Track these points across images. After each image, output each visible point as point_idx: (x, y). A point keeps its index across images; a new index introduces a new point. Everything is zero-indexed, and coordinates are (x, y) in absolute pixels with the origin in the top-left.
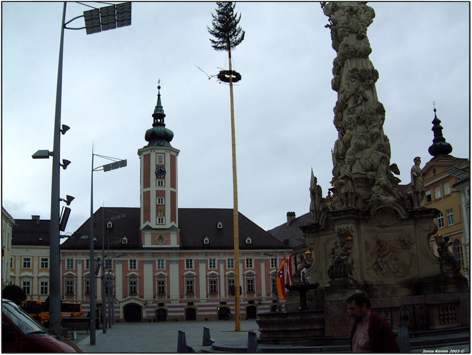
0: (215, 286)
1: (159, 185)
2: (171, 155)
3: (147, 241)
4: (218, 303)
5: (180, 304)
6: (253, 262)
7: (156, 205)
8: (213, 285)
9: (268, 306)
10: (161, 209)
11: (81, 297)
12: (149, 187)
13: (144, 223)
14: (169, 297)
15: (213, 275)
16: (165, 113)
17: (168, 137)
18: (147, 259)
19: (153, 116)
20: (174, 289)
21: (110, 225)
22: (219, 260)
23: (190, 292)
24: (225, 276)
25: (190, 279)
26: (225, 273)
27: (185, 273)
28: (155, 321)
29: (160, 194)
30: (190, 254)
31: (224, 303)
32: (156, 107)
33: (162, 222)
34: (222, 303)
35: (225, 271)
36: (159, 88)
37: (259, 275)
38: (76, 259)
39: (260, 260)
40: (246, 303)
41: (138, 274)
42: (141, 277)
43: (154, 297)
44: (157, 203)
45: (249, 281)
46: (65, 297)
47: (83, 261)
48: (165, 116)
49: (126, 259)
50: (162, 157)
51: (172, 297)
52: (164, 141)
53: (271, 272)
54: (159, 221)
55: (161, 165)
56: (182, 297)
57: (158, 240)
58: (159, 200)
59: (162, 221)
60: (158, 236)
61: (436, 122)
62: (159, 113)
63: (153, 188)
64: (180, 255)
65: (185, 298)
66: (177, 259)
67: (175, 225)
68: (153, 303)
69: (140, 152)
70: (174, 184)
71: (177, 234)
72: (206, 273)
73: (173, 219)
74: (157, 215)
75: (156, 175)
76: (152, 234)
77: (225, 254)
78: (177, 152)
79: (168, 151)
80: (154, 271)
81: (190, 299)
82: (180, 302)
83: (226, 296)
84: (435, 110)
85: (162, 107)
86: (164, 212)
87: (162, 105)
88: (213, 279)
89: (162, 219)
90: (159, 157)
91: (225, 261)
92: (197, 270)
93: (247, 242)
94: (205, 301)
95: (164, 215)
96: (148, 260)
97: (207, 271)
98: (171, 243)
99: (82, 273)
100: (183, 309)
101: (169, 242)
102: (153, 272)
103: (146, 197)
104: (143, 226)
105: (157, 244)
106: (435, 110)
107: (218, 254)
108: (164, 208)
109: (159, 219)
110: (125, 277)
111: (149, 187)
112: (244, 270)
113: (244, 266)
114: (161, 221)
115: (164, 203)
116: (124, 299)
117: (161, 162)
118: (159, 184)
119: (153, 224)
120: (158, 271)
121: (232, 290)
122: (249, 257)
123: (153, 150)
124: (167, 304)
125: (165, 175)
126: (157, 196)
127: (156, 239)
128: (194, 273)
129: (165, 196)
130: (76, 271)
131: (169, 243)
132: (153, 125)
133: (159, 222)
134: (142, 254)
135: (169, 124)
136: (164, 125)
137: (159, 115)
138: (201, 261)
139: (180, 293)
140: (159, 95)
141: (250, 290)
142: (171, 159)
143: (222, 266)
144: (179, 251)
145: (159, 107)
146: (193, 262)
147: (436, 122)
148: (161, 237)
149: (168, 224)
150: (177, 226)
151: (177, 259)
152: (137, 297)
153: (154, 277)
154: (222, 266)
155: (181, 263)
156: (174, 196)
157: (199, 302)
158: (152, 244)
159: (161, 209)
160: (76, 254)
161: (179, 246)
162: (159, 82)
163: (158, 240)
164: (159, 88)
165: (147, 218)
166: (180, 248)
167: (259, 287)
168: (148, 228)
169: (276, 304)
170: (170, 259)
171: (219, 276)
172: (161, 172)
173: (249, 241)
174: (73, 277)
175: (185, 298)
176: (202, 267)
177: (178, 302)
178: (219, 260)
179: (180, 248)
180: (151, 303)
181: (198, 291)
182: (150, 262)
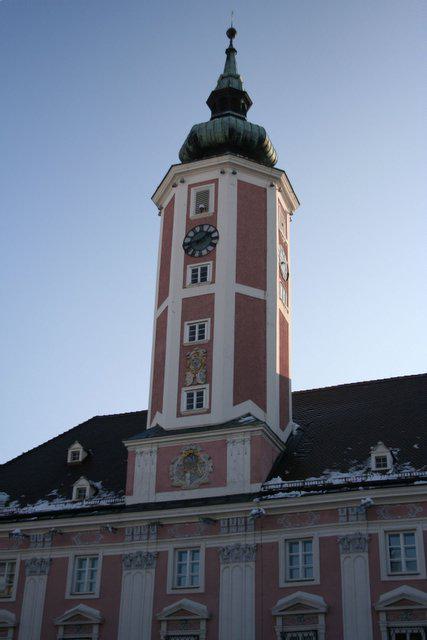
1: (194, 281)
33: (200, 405)
36: (231, 33)
41: (96, 612)
44: (186, 340)
50: (207, 193)
54: (190, 401)
58: (192, 328)
59: (200, 400)
63: (177, 294)
67: (257, 412)
72: (374, 598)
74: (182, 383)
75: (186, 251)
85: (238, 77)
87: (239, 72)
89: (200, 394)
90: (199, 195)
95: (208, 379)
96: (140, 554)
97: (377, 586)
98: (231, 475)
101: (219, 478)
105: (178, 488)
109: (190, 395)
114: (196, 402)
118: (194, 276)
125: (214, 245)
126: (184, 319)
127: (174, 469)
129: (211, 315)
131: (223, 482)
133: (190, 407)
134: (116, 533)
137: (229, 99)
140: (231, 51)
145: (230, 74)
151: (251, 540)
164: (231, 33)
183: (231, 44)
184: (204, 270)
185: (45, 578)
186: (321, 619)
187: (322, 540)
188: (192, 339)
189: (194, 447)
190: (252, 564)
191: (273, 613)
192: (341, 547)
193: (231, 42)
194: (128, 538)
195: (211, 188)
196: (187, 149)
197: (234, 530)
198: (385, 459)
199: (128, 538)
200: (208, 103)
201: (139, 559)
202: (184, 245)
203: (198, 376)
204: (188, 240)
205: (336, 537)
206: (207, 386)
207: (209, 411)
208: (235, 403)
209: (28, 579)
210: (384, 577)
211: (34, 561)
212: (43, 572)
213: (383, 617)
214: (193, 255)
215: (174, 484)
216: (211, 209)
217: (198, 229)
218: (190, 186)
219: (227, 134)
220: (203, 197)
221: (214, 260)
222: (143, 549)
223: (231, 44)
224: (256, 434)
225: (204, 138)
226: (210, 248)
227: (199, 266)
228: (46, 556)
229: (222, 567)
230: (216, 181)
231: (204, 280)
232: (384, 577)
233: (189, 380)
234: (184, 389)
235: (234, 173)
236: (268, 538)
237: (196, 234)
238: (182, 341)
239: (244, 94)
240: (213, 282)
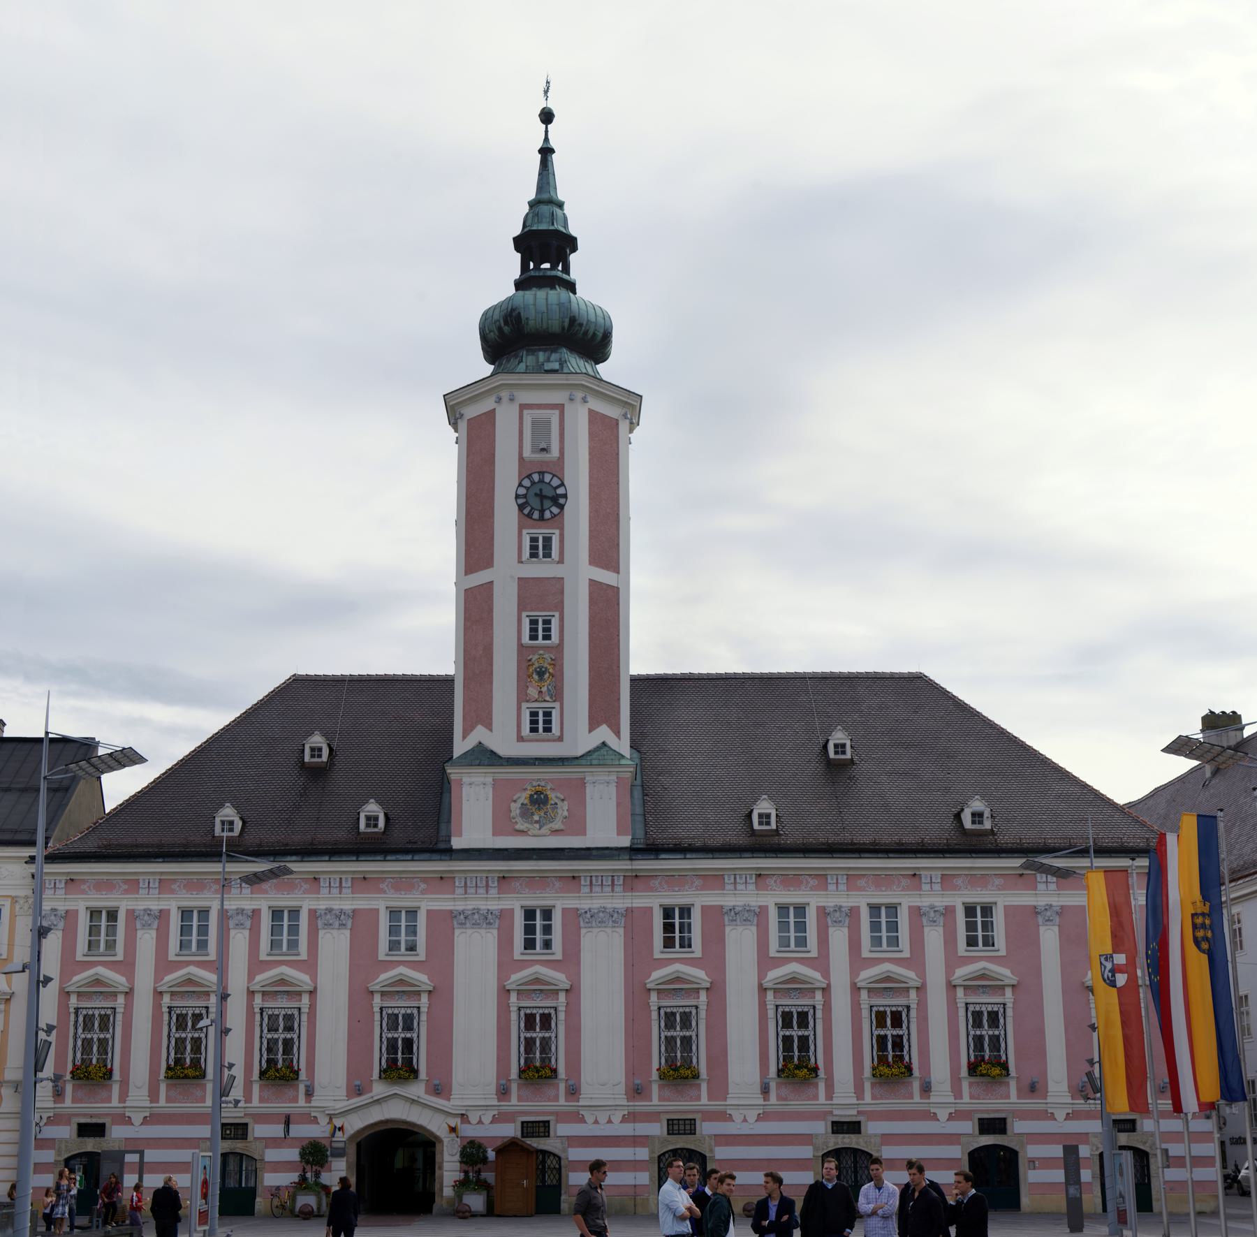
0: (804, 1041)
1: (534, 555)
2: (591, 411)
3: (475, 815)
4: (820, 1127)
5: (627, 1129)
6: (999, 919)
7: (521, 646)
8: (795, 1033)
10: (541, 671)
11: (145, 1091)
12: (489, 563)
13: (464, 737)
14: (573, 1092)
15: (793, 985)
16: (573, 230)
17: (591, 341)
18: (470, 905)
19: (519, 243)
20: (602, 1051)
21: (316, 751)
22: (823, 912)
23: (679, 1072)
24: (856, 989)
25: (676, 1003)
26: (854, 972)
27: (657, 975)
28: (482, 1216)
29: (541, 600)
30: (675, 880)
31: (853, 1127)
32: (532, 204)
33: (548, 729)
34: (839, 1127)
35: (857, 961)
36: (547, 117)
37: (1029, 987)
38: (132, 905)
39: (1035, 911)
41: (423, 978)
42: (442, 993)
43: (503, 1092)
44: (526, 639)
45: (977, 1016)
46: (69, 1089)
47: (163, 915)
48: (570, 243)
49: (373, 904)
50: (548, 422)
51: (591, 1092)
52: (565, 353)
54: (534, 722)
55: (543, 463)
56: (637, 1091)
57: (526, 813)
58: (534, 622)
59: (548, 722)
60: (523, 797)
62: (543, 227)
64: (633, 881)
65: (655, 1101)
66: (621, 901)
68: (494, 1120)
69: (455, 405)
70: (608, 547)
71: (619, 782)
72: (762, 974)
73: (602, 712)
74: (522, 697)
75: (521, 508)
76: (496, 784)
77: (852, 879)
78: (630, 403)
79: (579, 395)
80: (506, 964)
81: (680, 1106)
82: (631, 1117)
83: (859, 1092)
85: (560, 205)
86: (558, 677)
87: (561, 196)
88: (794, 1003)
89: (548, 714)
90: (534, 423)
91: (853, 912)
92: (715, 958)
93: (968, 824)
94: (752, 1115)
95: (557, 695)
96: (476, 911)
97: (765, 962)
99: (158, 977)
100: (643, 1154)
102: (500, 965)
103: (475, 610)
104: (460, 746)
105: (522, 832)
107: (822, 879)
108: (557, 662)
109: (534, 714)
110: (360, 995)
111: (489, 563)
112: (952, 961)
113: (950, 940)
114: (541, 723)
115: (555, 638)
116: (357, 1101)
117: (543, 450)
118: (534, 548)
119: (503, 736)
120: (524, 964)
123: (505, 394)
124: (562, 1129)
125: (562, 507)
126: (522, 607)
127: (515, 808)
128: (700, 974)
129: (560, 607)
130: (127, 966)
131: (582, 831)
132: (519, 285)
133: (534, 730)
135: (594, 281)
136: (571, 287)
138: (735, 914)
139: (631, 1071)
141: (986, 1064)
142: (592, 435)
143: (839, 938)
144: (624, 865)
145: (545, 200)
146: (696, 920)
148: (539, 800)
149: (579, 736)
150: (623, 745)
152: (416, 1090)
153: (504, 992)
154: (839, 938)
155: (633, 921)
156: (608, 611)
157: (724, 1117)
158: (496, 832)
159: (541, 671)
160: (133, 885)
161: (625, 841)
162: (546, 92)
163: (526, 813)
164: (547, 117)
165: (481, 714)
166: (633, 852)
167: (1035, 1048)
168: (484, 757)
170: (584, 904)
171: (826, 990)
172: (542, 499)
173: (978, 817)
174: (114, 995)
175: (655, 1101)
176: (740, 945)
177: (617, 1118)
178: (823, 912)
179: (633, 852)
180: (487, 1119)
181: (719, 1060)
182: (486, 919)
183: (546, 139)
184: (547, 540)
185: (347, 933)
186: (703, 996)
187: (704, 909)
188: (533, 637)
189: (543, 783)
190: (621, 931)
191: (649, 986)
192: (726, 918)
193: (546, 132)
194: (459, 891)
195: (554, 416)
196: (500, 329)
197: (598, 889)
198: (768, 816)
199: (459, 891)
200: (515, 239)
201: (476, 916)
202: (517, 497)
203: (544, 689)
204: (522, 491)
205: (722, 907)
206: (557, 705)
207: (560, 739)
208: (590, 731)
209: (321, 933)
210: (773, 953)
211: (330, 910)
212: (343, 925)
213: (770, 995)
214: (529, 516)
215: (518, 827)
216: (555, 452)
217: (536, 477)
218: (523, 407)
219: (566, 324)
220: (541, 428)
221: (562, 529)
222: (484, 906)
223: (546, 139)
224: (622, 775)
225: (531, 322)
226: (555, 510)
227: (540, 532)
228: (348, 906)
229: (583, 931)
230: (561, 407)
231: (547, 555)
232: (773, 953)
233: (533, 692)
234: (524, 705)
235: (584, 400)
236: (640, 900)
237: (533, 483)
238: (519, 639)
239: (575, 239)
240: (561, 561)
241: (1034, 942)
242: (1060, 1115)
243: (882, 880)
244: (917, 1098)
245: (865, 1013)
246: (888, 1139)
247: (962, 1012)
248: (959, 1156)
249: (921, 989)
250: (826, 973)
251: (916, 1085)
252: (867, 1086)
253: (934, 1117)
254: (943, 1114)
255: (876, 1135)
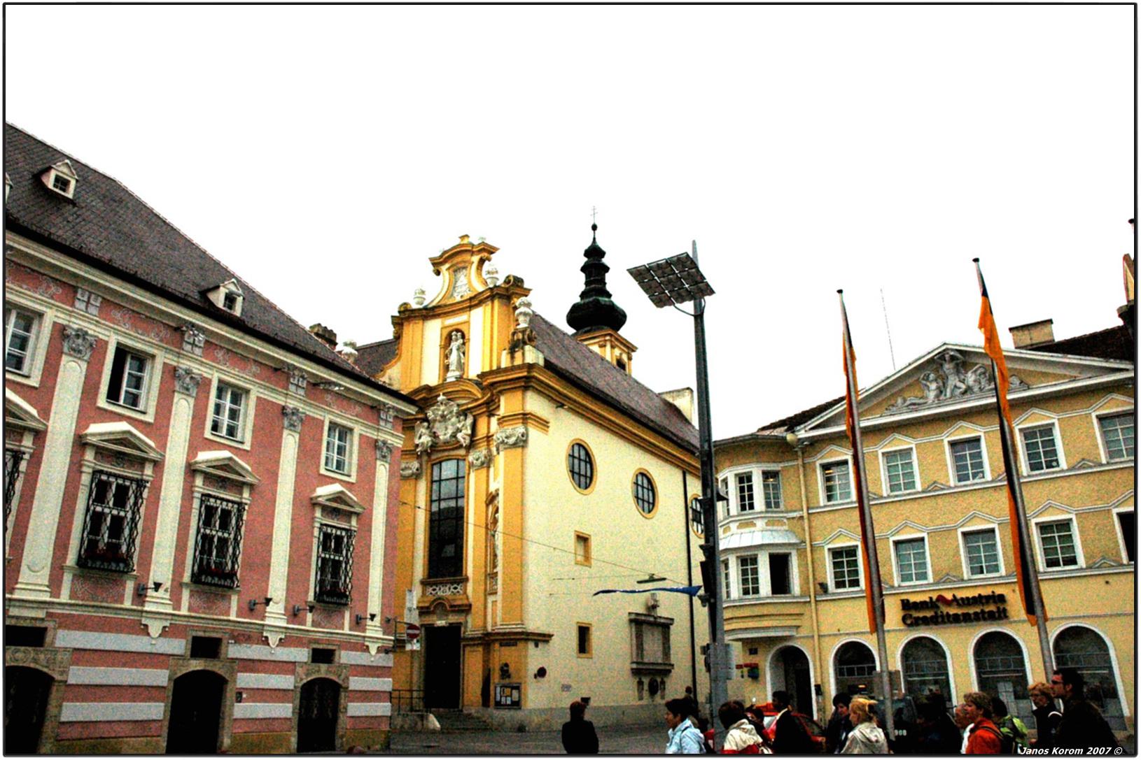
9: (285, 682)
24: (81, 443)
40: (178, 646)
53: (324, 491)
61: (594, 253)
77: (111, 303)
83: (55, 584)
84: (594, 228)
106: (594, 228)
107: (69, 288)
121: (105, 556)
122: (235, 376)
141: (213, 571)
147: (594, 253)
169: (323, 671)
178: (61, 333)
241: (276, 446)
242: (273, 639)
243: (142, 317)
244: (127, 604)
245: (86, 479)
246: (82, 655)
247: (196, 504)
248: (165, 684)
249: (158, 465)
250: (45, 412)
251: (130, 586)
252: (67, 578)
253: (145, 630)
254: (155, 628)
255: (65, 649)
